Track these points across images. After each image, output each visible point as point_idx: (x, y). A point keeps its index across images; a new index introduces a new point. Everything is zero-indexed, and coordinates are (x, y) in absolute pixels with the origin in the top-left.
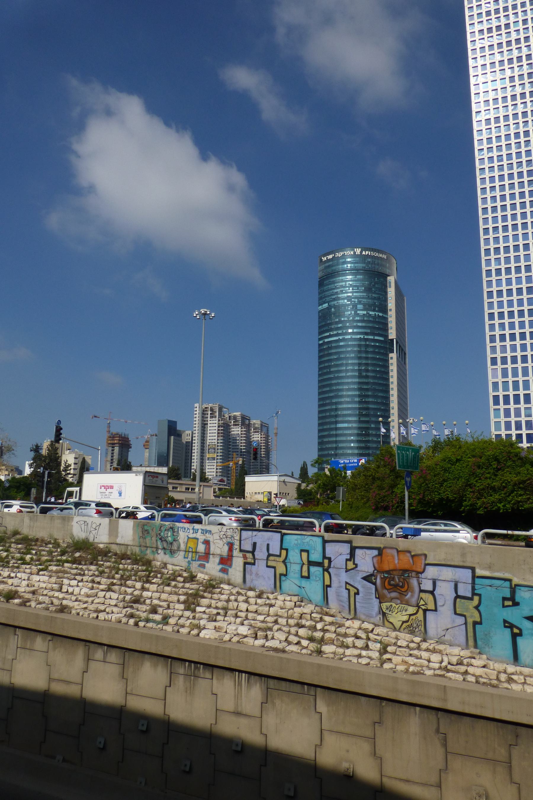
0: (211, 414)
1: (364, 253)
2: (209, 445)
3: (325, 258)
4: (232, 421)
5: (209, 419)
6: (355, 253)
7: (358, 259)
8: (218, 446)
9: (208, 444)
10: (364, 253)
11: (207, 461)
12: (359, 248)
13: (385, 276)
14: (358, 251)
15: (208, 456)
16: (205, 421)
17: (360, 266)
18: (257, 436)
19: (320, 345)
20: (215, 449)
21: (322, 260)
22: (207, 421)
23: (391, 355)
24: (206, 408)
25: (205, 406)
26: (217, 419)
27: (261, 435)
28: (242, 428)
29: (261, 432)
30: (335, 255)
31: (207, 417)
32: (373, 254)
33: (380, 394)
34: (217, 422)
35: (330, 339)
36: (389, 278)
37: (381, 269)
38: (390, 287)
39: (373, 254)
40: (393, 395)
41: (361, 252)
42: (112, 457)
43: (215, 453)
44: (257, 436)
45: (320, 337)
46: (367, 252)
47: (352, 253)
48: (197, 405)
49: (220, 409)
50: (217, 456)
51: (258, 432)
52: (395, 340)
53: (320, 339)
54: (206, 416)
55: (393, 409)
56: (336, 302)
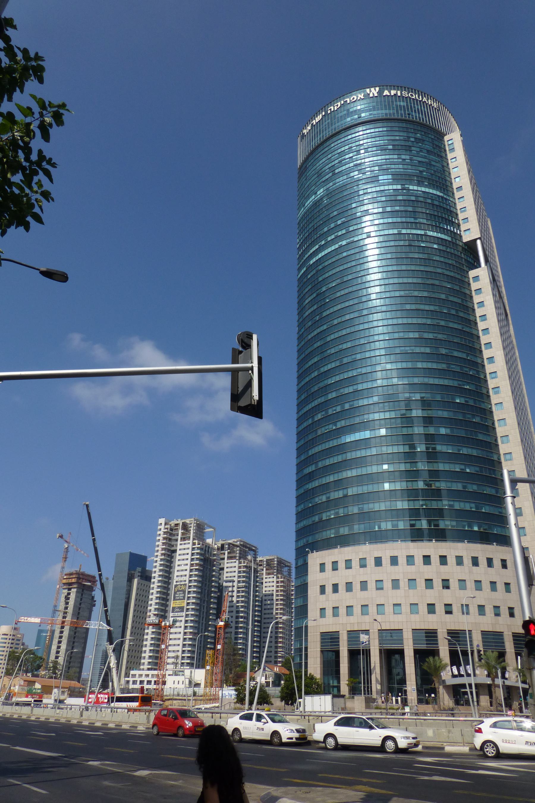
0: (183, 534)
1: (386, 93)
2: (176, 586)
3: (309, 128)
4: (226, 552)
5: (179, 542)
9: (175, 583)
11: (171, 614)
13: (441, 136)
14: (374, 92)
15: (172, 604)
16: (173, 546)
18: (271, 580)
20: (184, 592)
21: (303, 136)
22: (177, 545)
23: (472, 273)
24: (177, 525)
25: (173, 523)
27: (278, 578)
28: (240, 563)
30: (326, 112)
31: (177, 540)
32: (405, 94)
33: (456, 354)
35: (320, 256)
36: (446, 138)
37: (427, 121)
38: (452, 150)
39: (405, 94)
40: (491, 359)
41: (380, 93)
42: (64, 617)
43: (184, 597)
44: (271, 580)
46: (393, 92)
47: (361, 96)
48: (162, 521)
49: (200, 528)
50: (188, 604)
51: (273, 574)
52: (479, 242)
53: (299, 269)
54: (175, 537)
55: (497, 393)
56: (331, 184)
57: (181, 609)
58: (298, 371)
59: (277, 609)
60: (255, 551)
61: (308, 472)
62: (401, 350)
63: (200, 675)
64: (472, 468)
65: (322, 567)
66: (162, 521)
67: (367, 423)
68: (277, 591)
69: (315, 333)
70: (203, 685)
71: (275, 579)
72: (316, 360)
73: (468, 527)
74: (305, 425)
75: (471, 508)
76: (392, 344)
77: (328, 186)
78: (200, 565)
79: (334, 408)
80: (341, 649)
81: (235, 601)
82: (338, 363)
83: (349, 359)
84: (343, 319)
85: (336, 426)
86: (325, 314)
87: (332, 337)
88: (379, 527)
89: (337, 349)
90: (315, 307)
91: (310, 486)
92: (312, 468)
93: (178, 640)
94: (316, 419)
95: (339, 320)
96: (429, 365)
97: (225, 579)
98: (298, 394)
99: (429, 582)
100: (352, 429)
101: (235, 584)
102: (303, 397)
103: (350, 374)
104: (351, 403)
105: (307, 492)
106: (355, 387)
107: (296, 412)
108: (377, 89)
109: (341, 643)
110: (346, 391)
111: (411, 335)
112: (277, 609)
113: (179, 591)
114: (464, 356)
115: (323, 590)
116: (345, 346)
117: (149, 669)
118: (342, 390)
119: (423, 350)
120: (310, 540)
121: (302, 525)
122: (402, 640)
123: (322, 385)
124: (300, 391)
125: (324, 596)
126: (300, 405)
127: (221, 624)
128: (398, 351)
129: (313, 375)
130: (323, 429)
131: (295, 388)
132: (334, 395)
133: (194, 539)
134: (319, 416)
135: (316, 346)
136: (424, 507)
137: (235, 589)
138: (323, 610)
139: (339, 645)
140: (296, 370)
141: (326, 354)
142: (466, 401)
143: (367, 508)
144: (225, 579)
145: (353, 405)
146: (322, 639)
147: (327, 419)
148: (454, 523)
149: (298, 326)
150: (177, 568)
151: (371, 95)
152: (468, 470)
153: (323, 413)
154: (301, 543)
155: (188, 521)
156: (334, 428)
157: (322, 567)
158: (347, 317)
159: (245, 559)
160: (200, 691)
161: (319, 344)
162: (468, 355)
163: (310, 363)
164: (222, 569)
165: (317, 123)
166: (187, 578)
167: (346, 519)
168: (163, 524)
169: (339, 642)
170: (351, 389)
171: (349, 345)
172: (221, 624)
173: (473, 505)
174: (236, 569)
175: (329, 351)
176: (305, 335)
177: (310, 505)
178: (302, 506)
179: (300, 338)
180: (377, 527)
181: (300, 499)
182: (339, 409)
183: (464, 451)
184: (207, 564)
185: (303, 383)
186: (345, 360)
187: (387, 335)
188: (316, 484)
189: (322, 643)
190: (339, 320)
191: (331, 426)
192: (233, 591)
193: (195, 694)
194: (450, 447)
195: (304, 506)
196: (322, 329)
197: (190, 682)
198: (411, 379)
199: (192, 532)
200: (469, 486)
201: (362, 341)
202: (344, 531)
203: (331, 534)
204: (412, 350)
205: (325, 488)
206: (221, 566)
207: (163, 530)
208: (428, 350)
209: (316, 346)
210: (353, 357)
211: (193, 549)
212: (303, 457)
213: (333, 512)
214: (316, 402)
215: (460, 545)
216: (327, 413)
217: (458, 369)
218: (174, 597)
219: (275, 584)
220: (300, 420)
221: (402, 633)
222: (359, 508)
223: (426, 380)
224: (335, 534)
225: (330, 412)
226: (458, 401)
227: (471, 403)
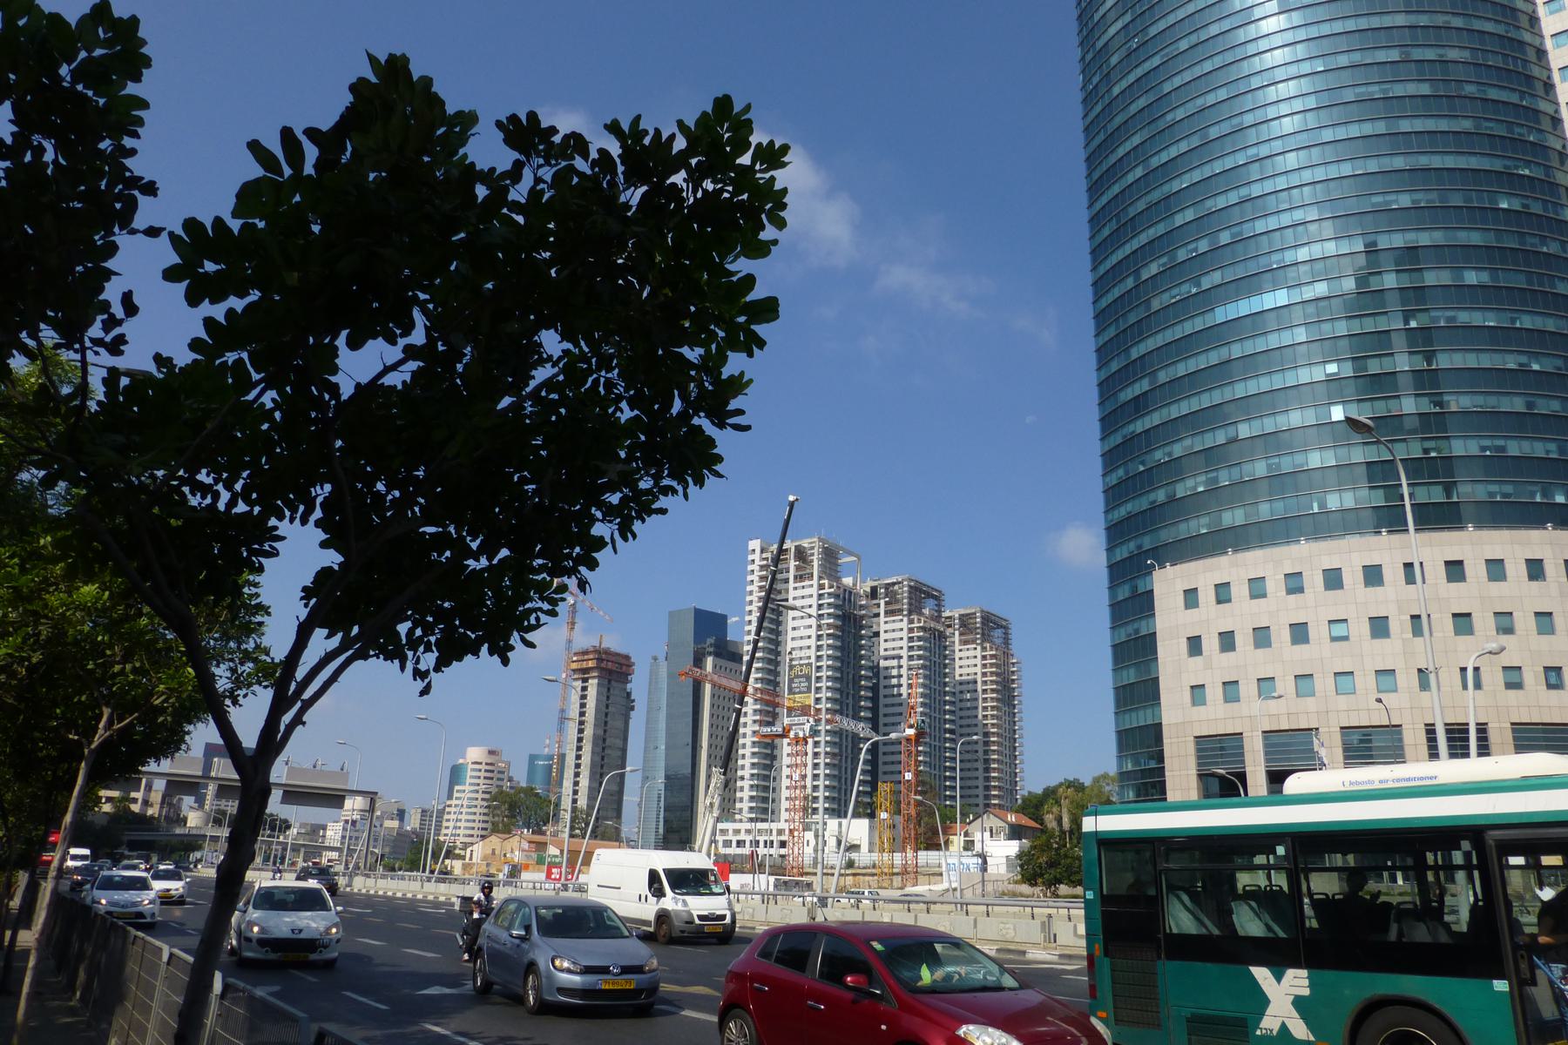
0: (798, 568)
4: (882, 602)
5: (791, 584)
8: (819, 668)
18: (971, 653)
20: (808, 678)
22: (787, 591)
26: (815, 582)
27: (984, 649)
28: (911, 622)
29: (984, 640)
31: (787, 581)
33: (1493, 94)
34: (814, 591)
42: (581, 731)
44: (971, 653)
48: (755, 544)
49: (830, 555)
51: (974, 642)
57: (805, 710)
58: (1089, 176)
59: (985, 708)
60: (938, 599)
61: (1130, 396)
62: (1357, 95)
63: (858, 829)
64: (1545, 360)
65: (1191, 598)
66: (755, 544)
67: (1281, 272)
68: (984, 674)
69: (1131, 78)
70: (865, 848)
71: (978, 652)
72: (1136, 140)
73: (1544, 495)
74: (1117, 292)
75: (1548, 452)
76: (1332, 80)
78: (836, 627)
79: (1191, 247)
80: (1248, 769)
81: (905, 695)
82: (1195, 141)
83: (1225, 128)
84: (1203, 36)
85: (1198, 285)
86: (1153, 31)
87: (1177, 81)
88: (1322, 505)
89: (1191, 108)
90: (1128, 18)
91: (1139, 426)
92: (1145, 385)
93: (802, 768)
94: (1144, 277)
95: (1193, 39)
96: (1431, 125)
97: (882, 653)
98: (1092, 228)
99: (1463, 621)
100: (1250, 284)
101: (904, 662)
102: (1106, 232)
103: (1229, 163)
104: (1237, 229)
105: (1131, 440)
106: (1244, 192)
107: (1089, 267)
109: (1248, 758)
110: (1221, 202)
111: (1382, 56)
112: (985, 708)
113: (798, 677)
114: (1514, 98)
115: (1195, 645)
116: (1211, 99)
117: (751, 820)
118: (1209, 203)
119: (1412, 89)
120: (1147, 542)
121: (1122, 512)
122: (1402, 748)
123: (1156, 196)
124: (1096, 221)
125: (1198, 659)
126: (1098, 253)
127: (911, 732)
128: (1349, 95)
129: (1130, 178)
130: (1166, 296)
131: (1084, 215)
132: (1189, 215)
133: (820, 578)
134: (1154, 269)
135: (1134, 108)
136: (1433, 454)
137: (904, 671)
138: (1197, 689)
139: (1243, 762)
140: (1084, 173)
141: (1161, 125)
142: (1524, 206)
143: (1287, 464)
144: (882, 653)
145: (1241, 233)
146: (1198, 750)
147: (1174, 272)
148: (1509, 489)
149: (1083, 72)
150: (791, 634)
152: (1536, 367)
153: (1164, 260)
154: (1122, 553)
155: (805, 544)
156: (1194, 291)
157: (1191, 598)
158: (1214, 30)
159: (920, 614)
160: (864, 857)
161: (1142, 103)
162: (1522, 94)
163: (1121, 152)
164: (877, 634)
166: (812, 653)
167: (1242, 490)
168: (758, 551)
169: (1242, 754)
170: (1233, 198)
171: (1222, 94)
172: (911, 732)
173: (1552, 446)
174: (904, 634)
175: (1169, 117)
176: (1102, 90)
177: (1142, 468)
178: (1121, 472)
179: (1088, 100)
180: (1315, 505)
181: (1111, 459)
182: (1203, 246)
183: (1526, 322)
184: (850, 626)
185: (1104, 200)
186: (1214, 132)
187: (1320, 61)
188: (1155, 419)
189: (1199, 758)
190: (1193, 39)
191: (1185, 288)
192: (900, 676)
193: (850, 864)
194: (1490, 315)
195: (1127, 472)
196: (1147, 66)
197: (839, 843)
198: (1386, 160)
199: (816, 564)
200: (1540, 401)
201: (1256, 82)
202: (1234, 517)
203: (1201, 525)
204: (1384, 91)
205: (1171, 429)
206: (875, 629)
207: (758, 562)
208: (1425, 89)
209: (1134, 108)
210: (1235, 121)
211: (820, 596)
212: (1115, 366)
213: (1202, 478)
214: (1143, 239)
215: (1535, 535)
216: (1173, 258)
217: (1501, 131)
218: (791, 691)
219: (978, 661)
220: (1100, 286)
221: (1400, 733)
222: (1269, 466)
223: (1424, 161)
224: (1208, 526)
225: (1182, 255)
226: (1505, 206)
227: (1536, 208)
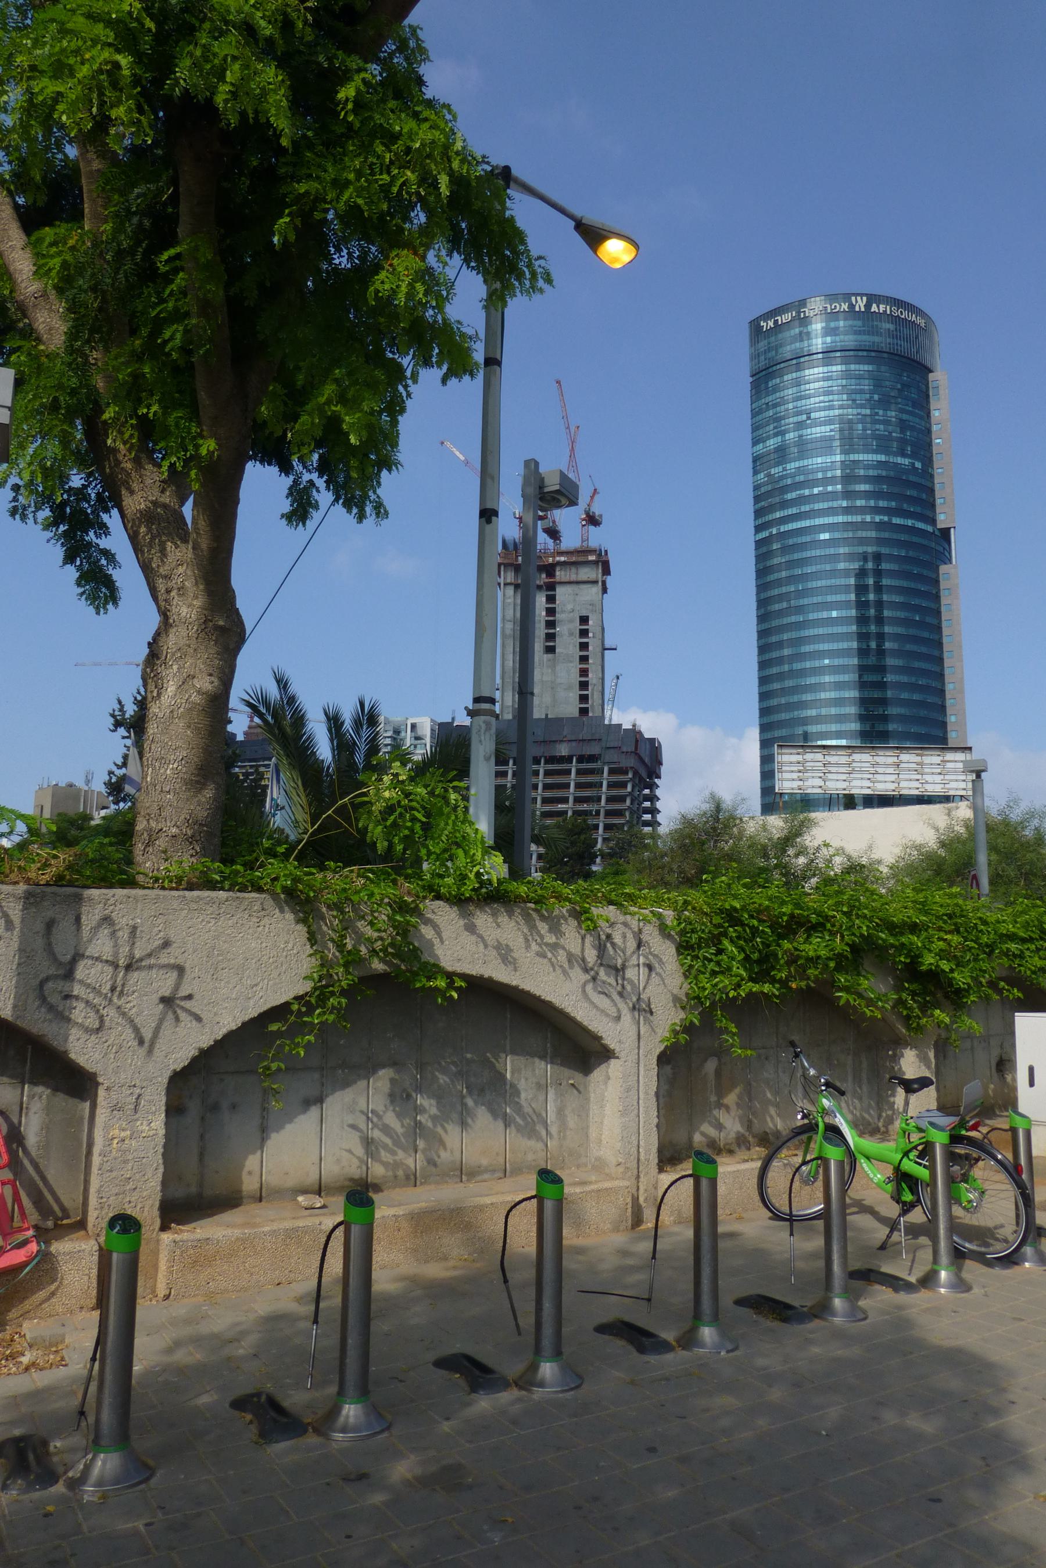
1: (874, 308)
3: (771, 324)
6: (852, 306)
7: (859, 323)
10: (874, 308)
12: (862, 295)
17: (867, 339)
19: (759, 544)
30: (799, 313)
41: (868, 306)
45: (760, 521)
46: (882, 307)
47: (845, 307)
77: (800, 432)
108: (865, 299)
151: (857, 309)
165: (782, 324)
